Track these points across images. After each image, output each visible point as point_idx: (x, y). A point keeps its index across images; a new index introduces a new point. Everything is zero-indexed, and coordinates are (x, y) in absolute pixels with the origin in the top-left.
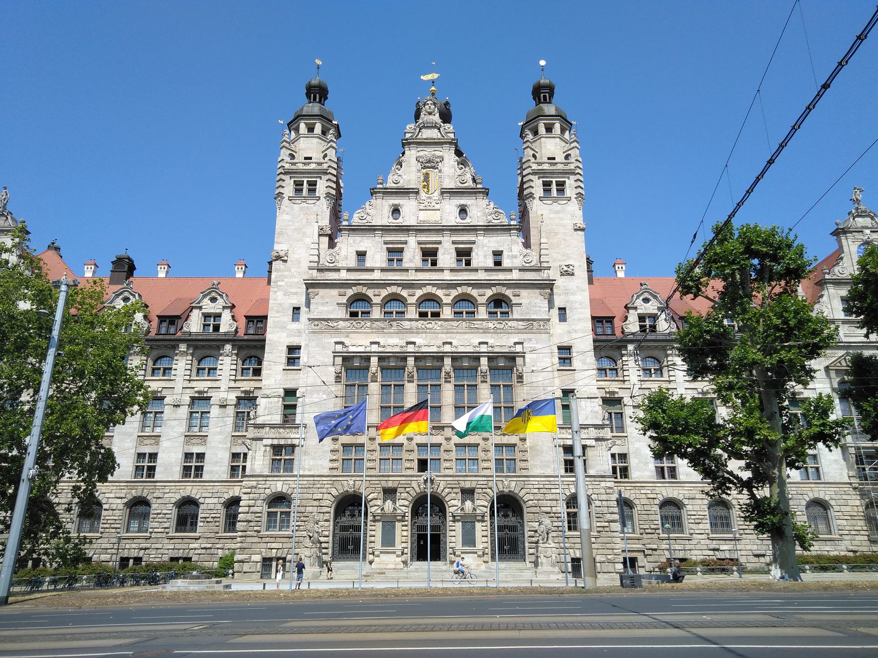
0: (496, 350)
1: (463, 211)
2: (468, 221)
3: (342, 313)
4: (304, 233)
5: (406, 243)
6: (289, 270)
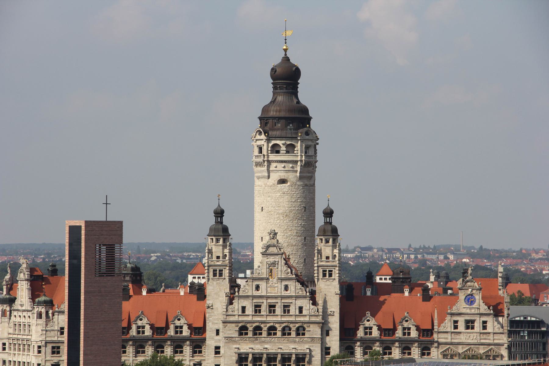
0: (299, 351)
1: (286, 288)
2: (287, 293)
3: (236, 335)
4: (219, 295)
5: (263, 303)
6: (214, 313)
